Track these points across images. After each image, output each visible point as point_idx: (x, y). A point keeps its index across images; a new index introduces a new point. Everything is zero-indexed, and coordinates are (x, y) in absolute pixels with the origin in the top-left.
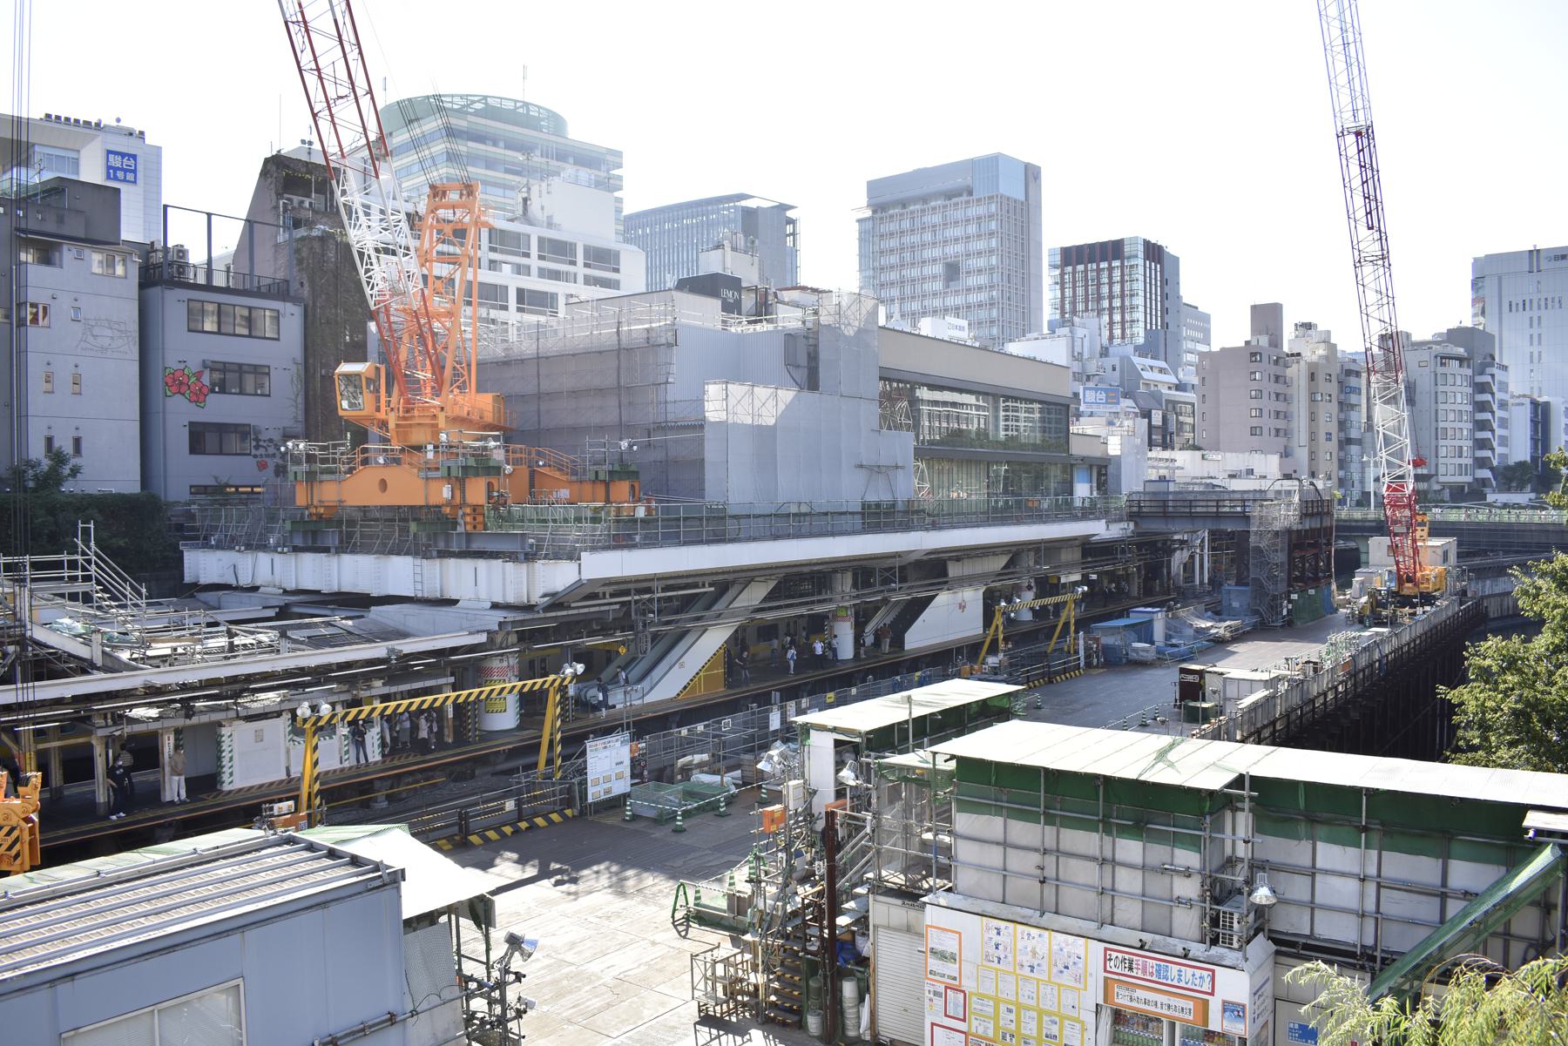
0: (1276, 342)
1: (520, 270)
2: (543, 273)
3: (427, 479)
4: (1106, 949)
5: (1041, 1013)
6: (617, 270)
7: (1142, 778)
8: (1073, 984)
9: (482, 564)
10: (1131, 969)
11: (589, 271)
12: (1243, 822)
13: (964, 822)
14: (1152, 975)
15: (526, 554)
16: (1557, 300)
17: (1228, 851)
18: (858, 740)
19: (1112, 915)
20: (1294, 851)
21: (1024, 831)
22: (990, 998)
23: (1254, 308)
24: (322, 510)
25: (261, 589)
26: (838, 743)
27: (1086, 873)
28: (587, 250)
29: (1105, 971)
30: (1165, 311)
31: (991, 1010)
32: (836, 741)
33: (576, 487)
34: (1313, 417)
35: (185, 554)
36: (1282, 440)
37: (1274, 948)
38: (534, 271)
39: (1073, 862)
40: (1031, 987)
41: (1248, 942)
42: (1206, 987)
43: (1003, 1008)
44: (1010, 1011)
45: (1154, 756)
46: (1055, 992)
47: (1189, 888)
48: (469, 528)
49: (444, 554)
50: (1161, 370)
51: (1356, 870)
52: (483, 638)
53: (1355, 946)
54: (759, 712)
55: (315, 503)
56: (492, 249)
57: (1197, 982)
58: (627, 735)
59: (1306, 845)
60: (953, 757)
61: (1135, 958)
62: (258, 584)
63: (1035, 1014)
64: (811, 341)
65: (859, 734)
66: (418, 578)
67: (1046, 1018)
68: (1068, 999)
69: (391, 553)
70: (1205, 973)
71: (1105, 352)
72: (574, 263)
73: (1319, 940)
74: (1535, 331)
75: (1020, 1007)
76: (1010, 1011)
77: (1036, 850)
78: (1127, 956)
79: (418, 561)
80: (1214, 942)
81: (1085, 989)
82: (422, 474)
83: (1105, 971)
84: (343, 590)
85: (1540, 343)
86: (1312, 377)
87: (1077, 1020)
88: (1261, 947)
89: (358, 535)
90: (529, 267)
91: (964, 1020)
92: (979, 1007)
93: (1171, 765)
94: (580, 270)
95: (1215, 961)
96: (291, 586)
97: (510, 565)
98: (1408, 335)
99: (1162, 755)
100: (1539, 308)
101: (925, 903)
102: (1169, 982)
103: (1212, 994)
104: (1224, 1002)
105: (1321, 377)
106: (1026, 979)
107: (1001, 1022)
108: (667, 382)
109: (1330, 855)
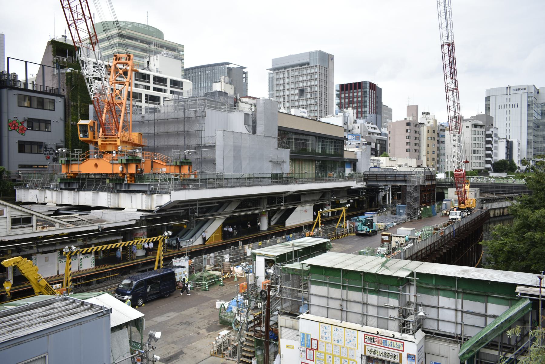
1: (148, 88)
2: (155, 89)
3: (113, 164)
4: (365, 335)
5: (341, 358)
6: (182, 89)
7: (377, 273)
8: (353, 347)
10: (374, 342)
11: (172, 89)
12: (413, 289)
13: (314, 289)
14: (381, 344)
15: (150, 191)
17: (408, 300)
18: (273, 259)
19: (367, 322)
20: (431, 299)
21: (336, 293)
22: (323, 353)
24: (72, 175)
26: (266, 260)
27: (358, 308)
28: (171, 80)
29: (365, 342)
31: (323, 357)
32: (265, 259)
33: (169, 167)
37: (425, 334)
38: (152, 88)
39: (353, 304)
40: (336, 349)
41: (416, 332)
42: (401, 349)
43: (327, 356)
44: (330, 357)
45: (381, 265)
46: (346, 350)
47: (394, 314)
48: (129, 182)
49: (119, 192)
51: (454, 307)
52: (134, 222)
53: (454, 334)
54: (235, 249)
55: (70, 172)
56: (136, 80)
57: (398, 347)
58: (187, 257)
59: (435, 297)
60: (309, 265)
61: (375, 338)
63: (339, 359)
64: (254, 116)
65: (274, 257)
67: (343, 360)
68: (351, 353)
69: (98, 191)
70: (401, 343)
72: (166, 86)
73: (441, 331)
75: (334, 356)
76: (330, 357)
77: (339, 299)
78: (372, 337)
80: (404, 332)
81: (357, 349)
82: (111, 162)
83: (365, 342)
84: (80, 204)
87: (354, 361)
88: (420, 334)
89: (86, 184)
90: (150, 87)
91: (313, 361)
92: (319, 356)
93: (387, 268)
94: (169, 88)
95: (404, 339)
96: (60, 203)
97: (144, 196)
99: (383, 265)
101: (299, 318)
102: (388, 347)
103: (403, 351)
104: (408, 354)
106: (336, 346)
107: (327, 362)
108: (202, 130)
109: (445, 301)
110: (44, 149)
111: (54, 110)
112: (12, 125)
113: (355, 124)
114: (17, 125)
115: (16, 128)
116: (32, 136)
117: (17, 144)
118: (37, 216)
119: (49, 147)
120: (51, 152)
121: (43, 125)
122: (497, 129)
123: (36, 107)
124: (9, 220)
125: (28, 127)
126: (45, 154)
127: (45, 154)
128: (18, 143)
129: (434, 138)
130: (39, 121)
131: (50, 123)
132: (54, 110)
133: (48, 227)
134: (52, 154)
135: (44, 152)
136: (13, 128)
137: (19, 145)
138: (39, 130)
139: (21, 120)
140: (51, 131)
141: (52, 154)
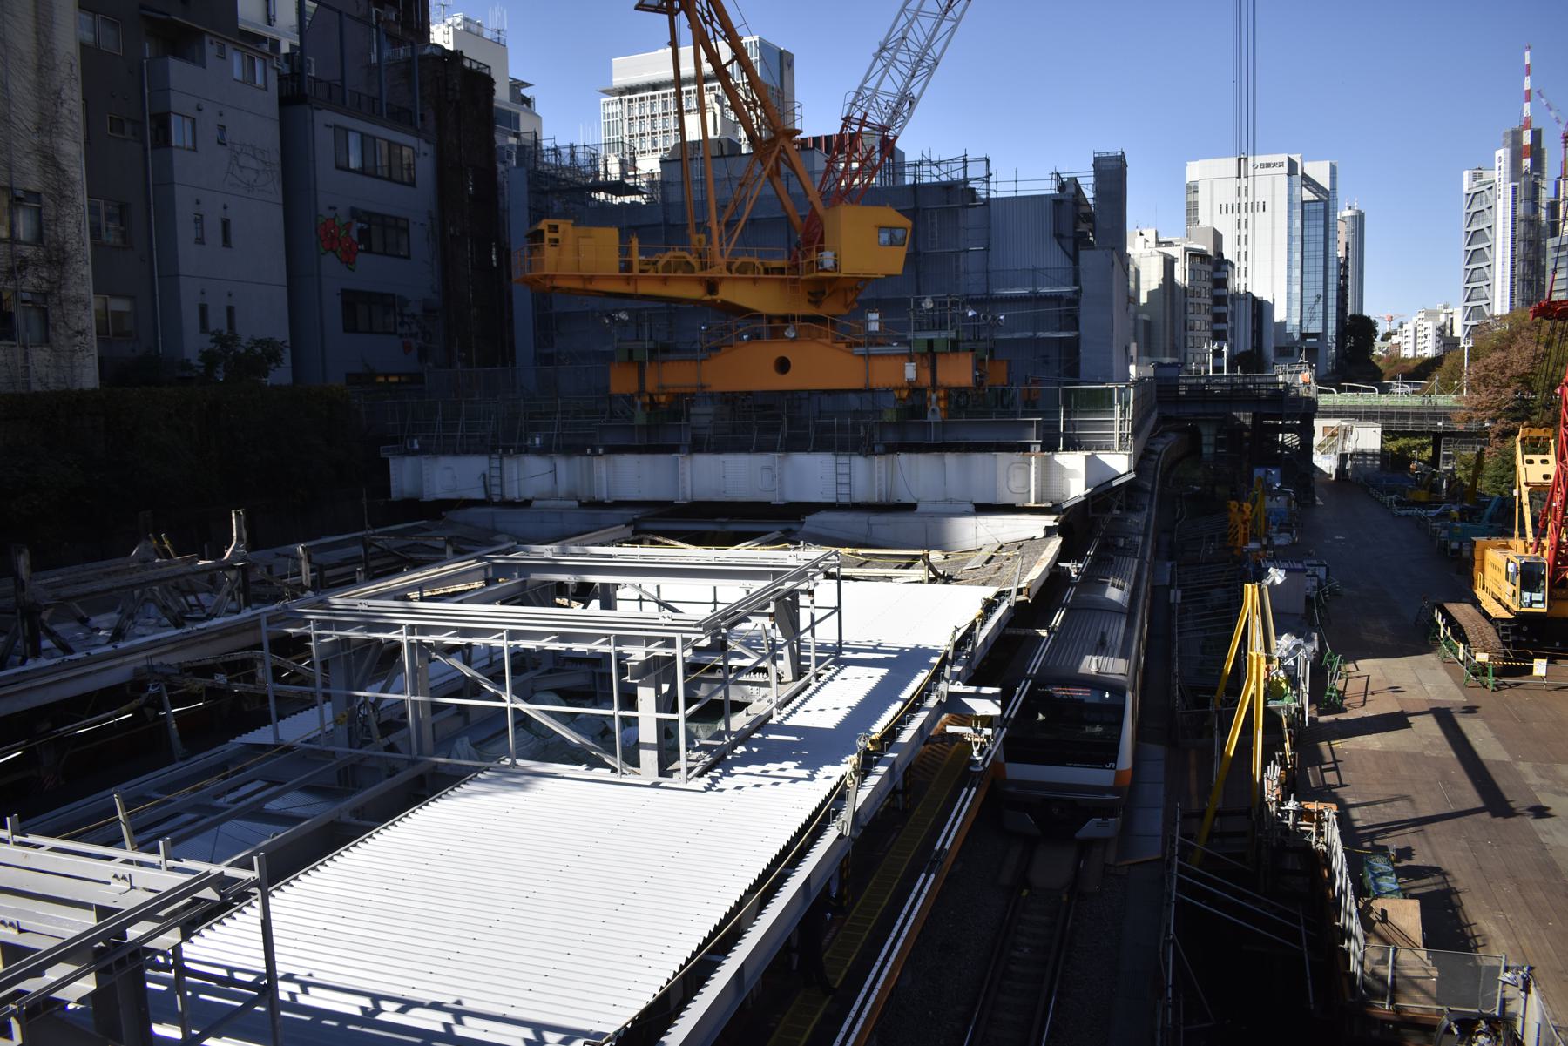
9: (951, 459)
25: (535, 503)
35: (391, 462)
62: (528, 495)
66: (845, 480)
79: (844, 459)
82: (861, 350)
100: (1246, 211)
110: (399, 319)
116: (372, 272)
120: (415, 329)
125: (360, 242)
126: (401, 336)
127: (401, 336)
128: (340, 297)
131: (406, 230)
135: (400, 330)
138: (384, 254)
140: (408, 257)
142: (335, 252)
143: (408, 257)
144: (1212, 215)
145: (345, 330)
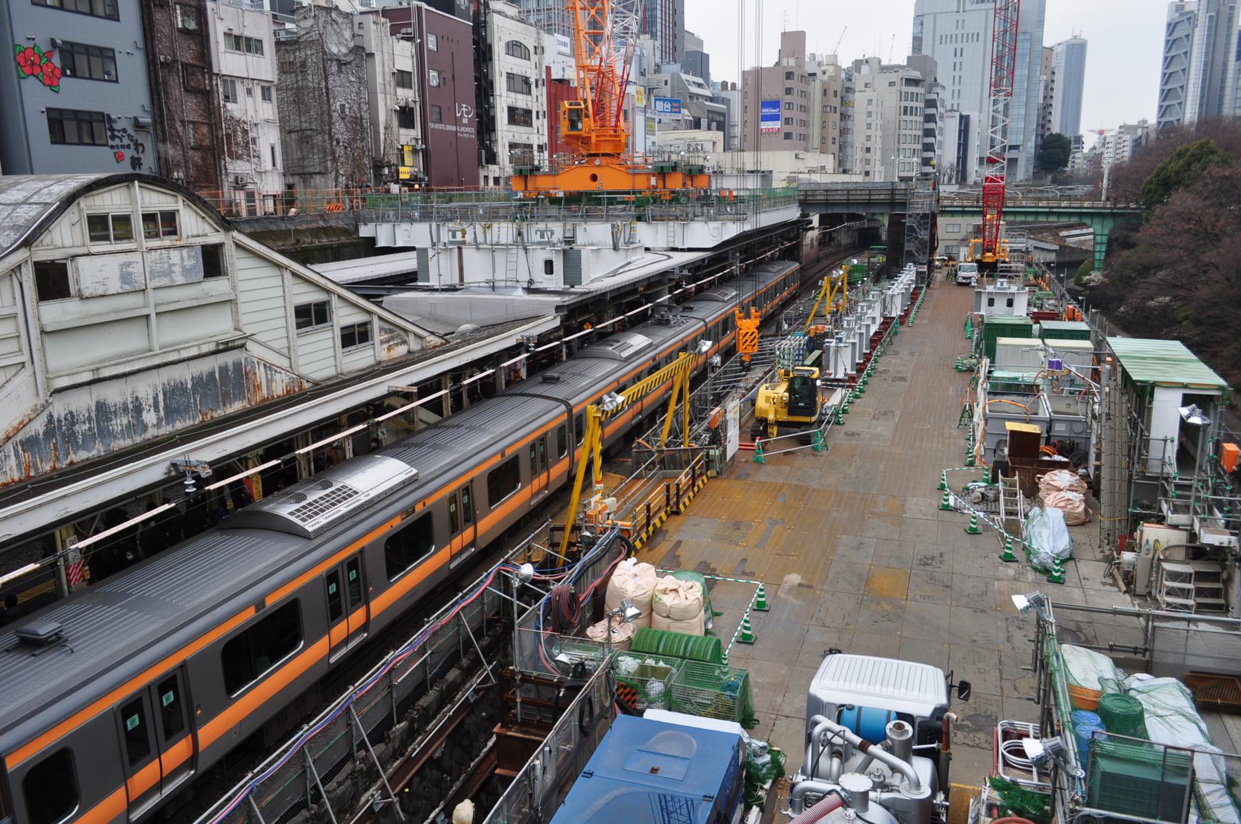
0: (801, 64)
16: (975, 35)
23: (784, 34)
30: (675, 36)
34: (824, 125)
36: (803, 143)
50: (700, 85)
71: (658, 69)
74: (958, 59)
85: (960, 69)
86: (825, 92)
98: (880, 62)
100: (962, 41)
105: (831, 93)
110: (109, 133)
111: (118, 20)
112: (26, 60)
113: (656, 76)
114: (37, 61)
115: (36, 70)
117: (44, 118)
118: (381, 318)
119: (117, 126)
120: (126, 141)
121: (96, 63)
122: (943, 87)
123: (74, 9)
124: (338, 333)
126: (112, 147)
127: (112, 147)
129: (835, 108)
130: (88, 50)
131: (113, 59)
132: (118, 20)
133: (397, 344)
134: (128, 146)
135: (110, 143)
136: (27, 69)
137: (49, 120)
138: (91, 78)
139: (45, 47)
140: (117, 81)
141: (128, 146)
142: (37, 77)
143: (117, 81)
144: (934, 44)
145: (54, 141)
